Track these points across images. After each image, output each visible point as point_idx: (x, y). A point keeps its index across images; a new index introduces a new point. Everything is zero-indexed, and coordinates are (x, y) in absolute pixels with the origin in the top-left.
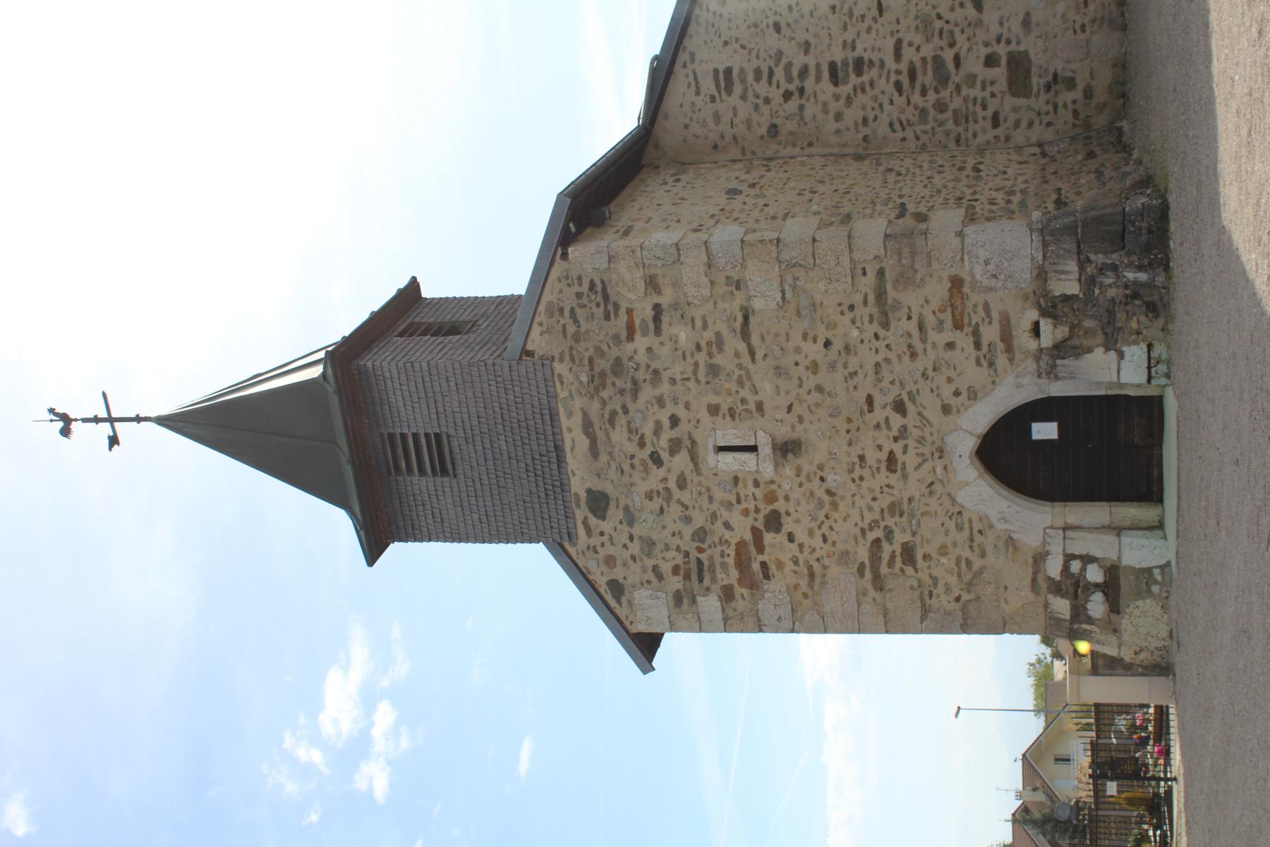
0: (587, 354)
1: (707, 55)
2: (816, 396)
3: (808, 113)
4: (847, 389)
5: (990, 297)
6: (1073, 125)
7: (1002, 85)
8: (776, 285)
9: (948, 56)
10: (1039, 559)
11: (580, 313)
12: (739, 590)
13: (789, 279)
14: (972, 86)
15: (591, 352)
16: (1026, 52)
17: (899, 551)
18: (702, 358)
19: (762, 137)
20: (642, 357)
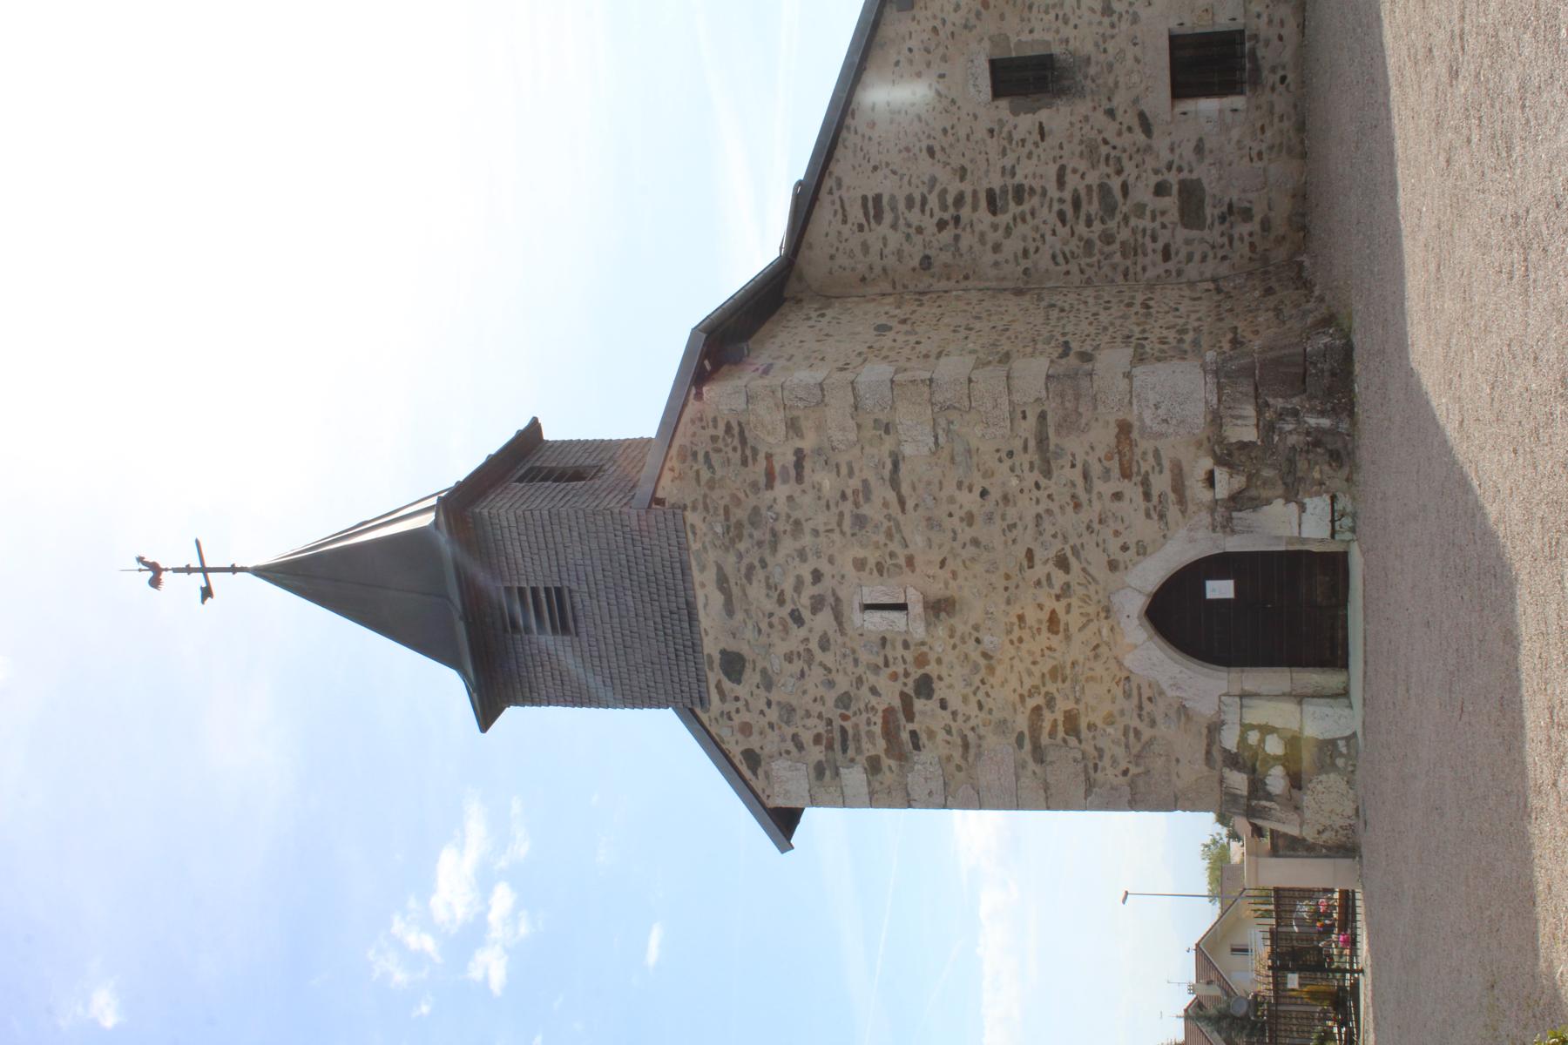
0: (722, 503)
1: (853, 180)
2: (971, 550)
3: (964, 244)
4: (1006, 543)
5: (1159, 444)
6: (1250, 259)
7: (1174, 215)
8: (928, 429)
9: (1115, 184)
10: (1214, 729)
11: (714, 457)
12: (886, 762)
13: (943, 422)
14: (1141, 215)
15: (727, 500)
16: (1199, 180)
17: (1061, 719)
18: (847, 507)
19: (914, 269)
20: (782, 506)
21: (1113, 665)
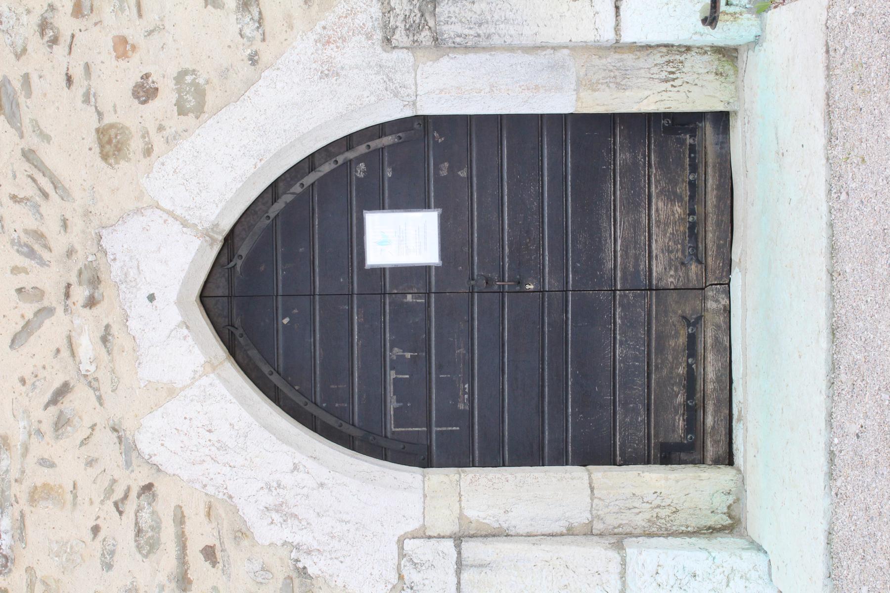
21: (106, 446)
